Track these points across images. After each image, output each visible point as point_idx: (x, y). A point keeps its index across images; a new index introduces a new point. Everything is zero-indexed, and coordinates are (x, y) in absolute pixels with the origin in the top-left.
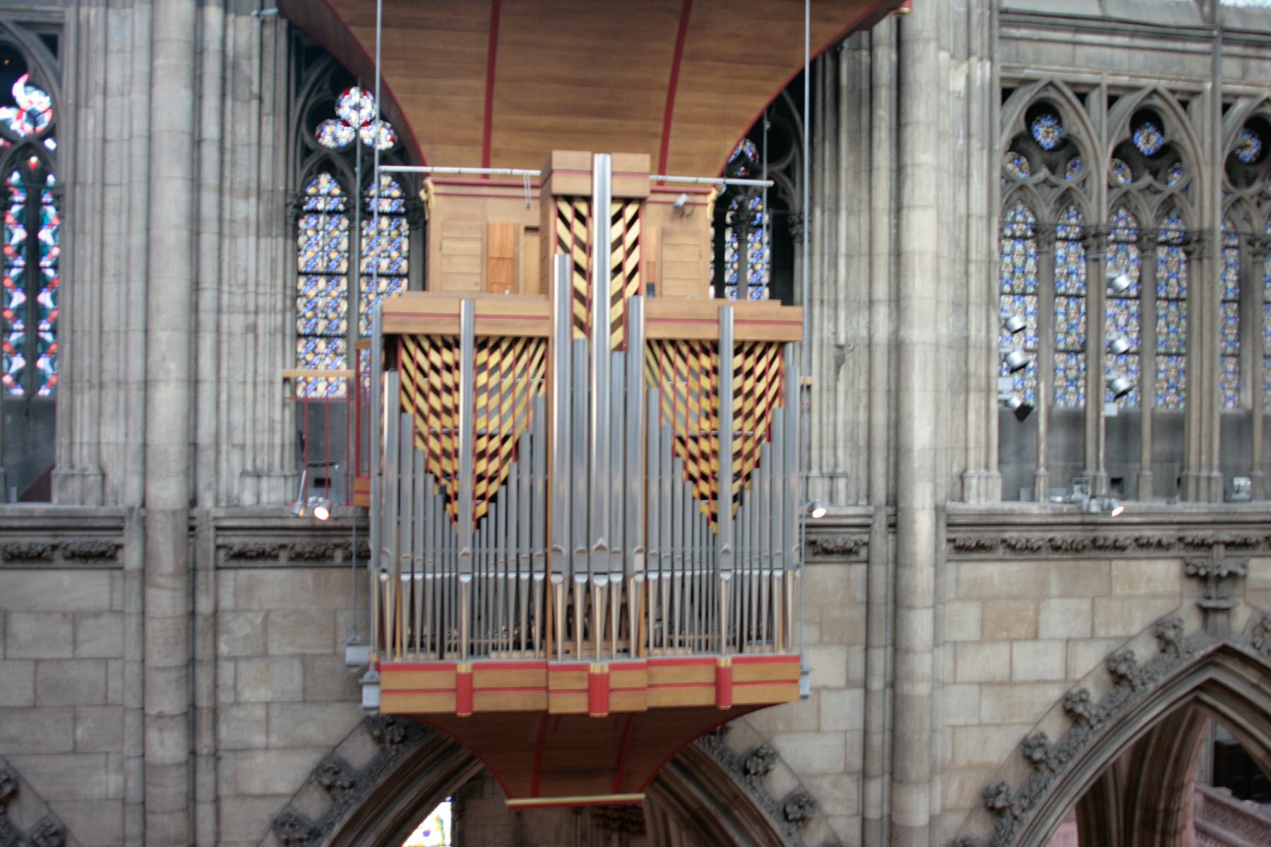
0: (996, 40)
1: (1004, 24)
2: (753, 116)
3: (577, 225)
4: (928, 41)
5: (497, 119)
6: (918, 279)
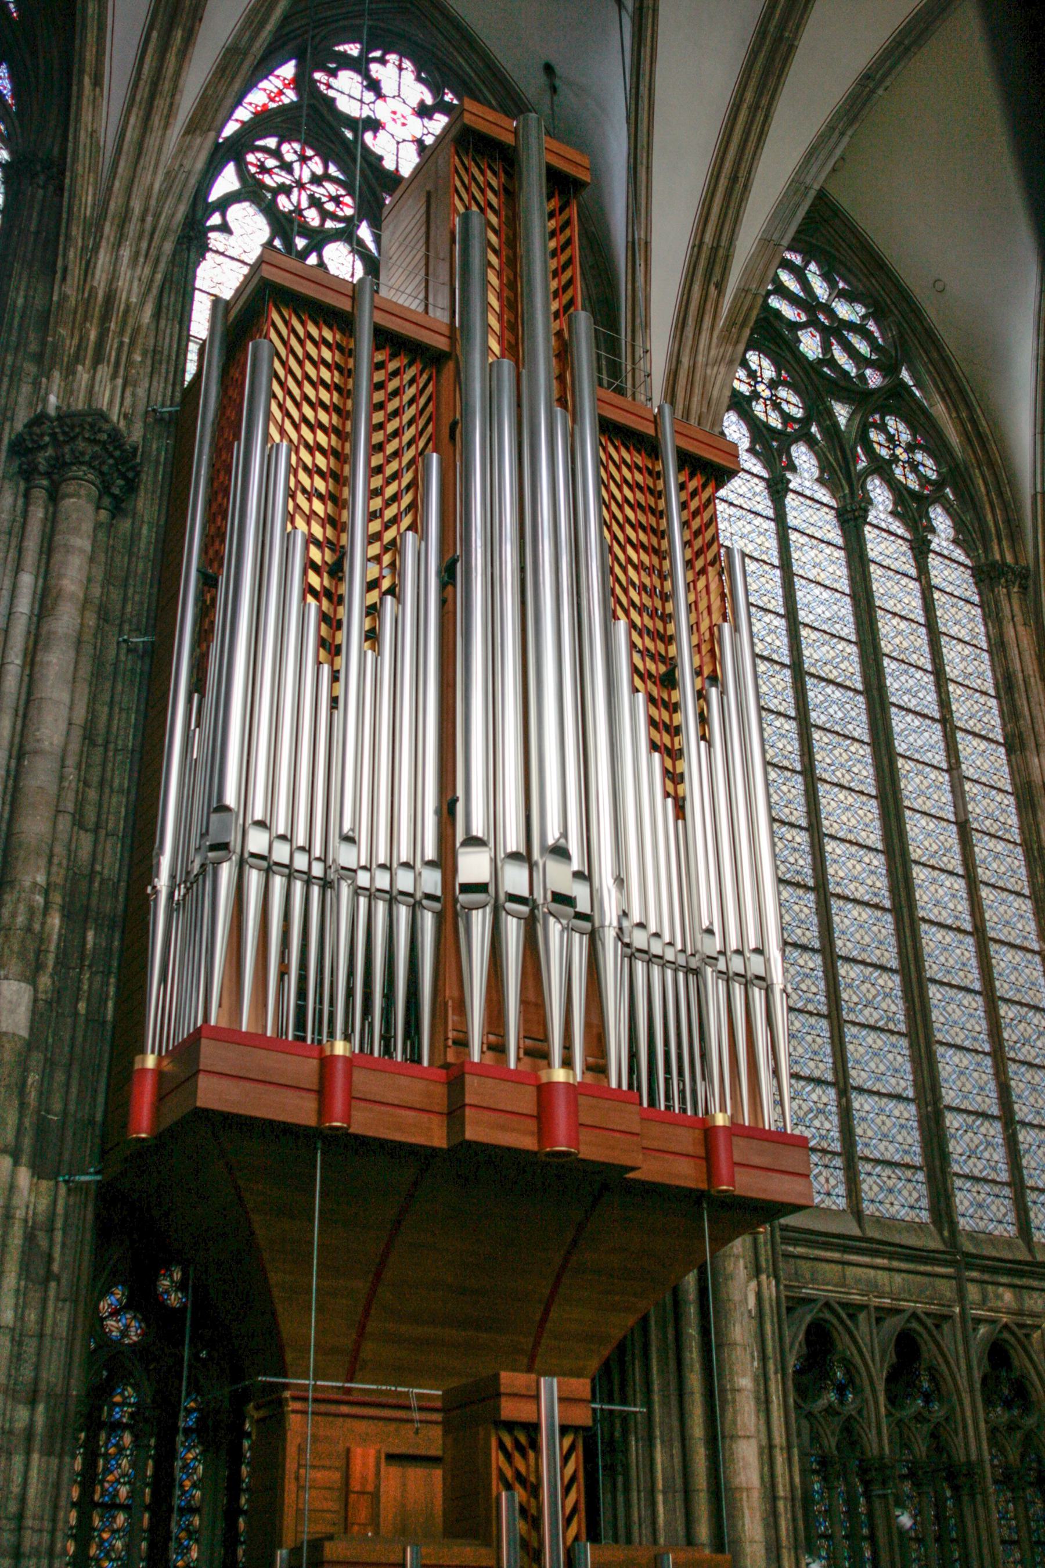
0: (780, 1259)
1: (786, 1241)
2: (617, 1334)
3: (517, 1456)
4: (737, 1257)
5: (371, 1326)
6: (747, 1520)
